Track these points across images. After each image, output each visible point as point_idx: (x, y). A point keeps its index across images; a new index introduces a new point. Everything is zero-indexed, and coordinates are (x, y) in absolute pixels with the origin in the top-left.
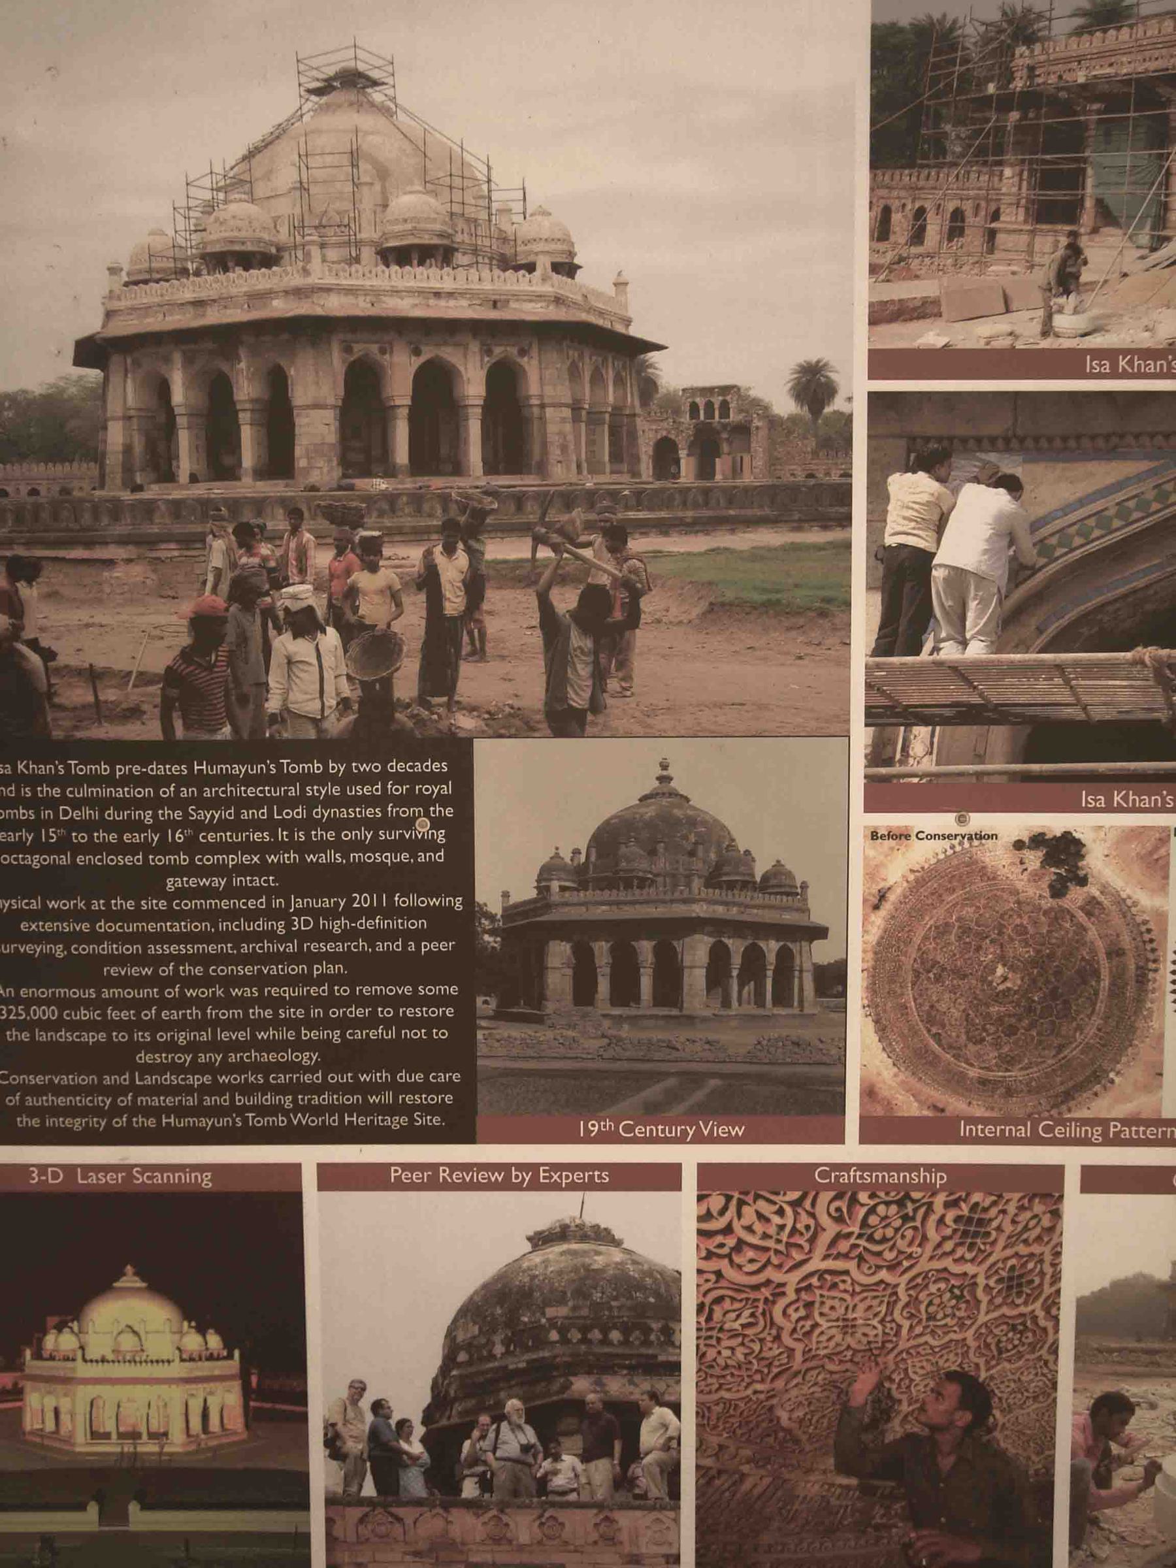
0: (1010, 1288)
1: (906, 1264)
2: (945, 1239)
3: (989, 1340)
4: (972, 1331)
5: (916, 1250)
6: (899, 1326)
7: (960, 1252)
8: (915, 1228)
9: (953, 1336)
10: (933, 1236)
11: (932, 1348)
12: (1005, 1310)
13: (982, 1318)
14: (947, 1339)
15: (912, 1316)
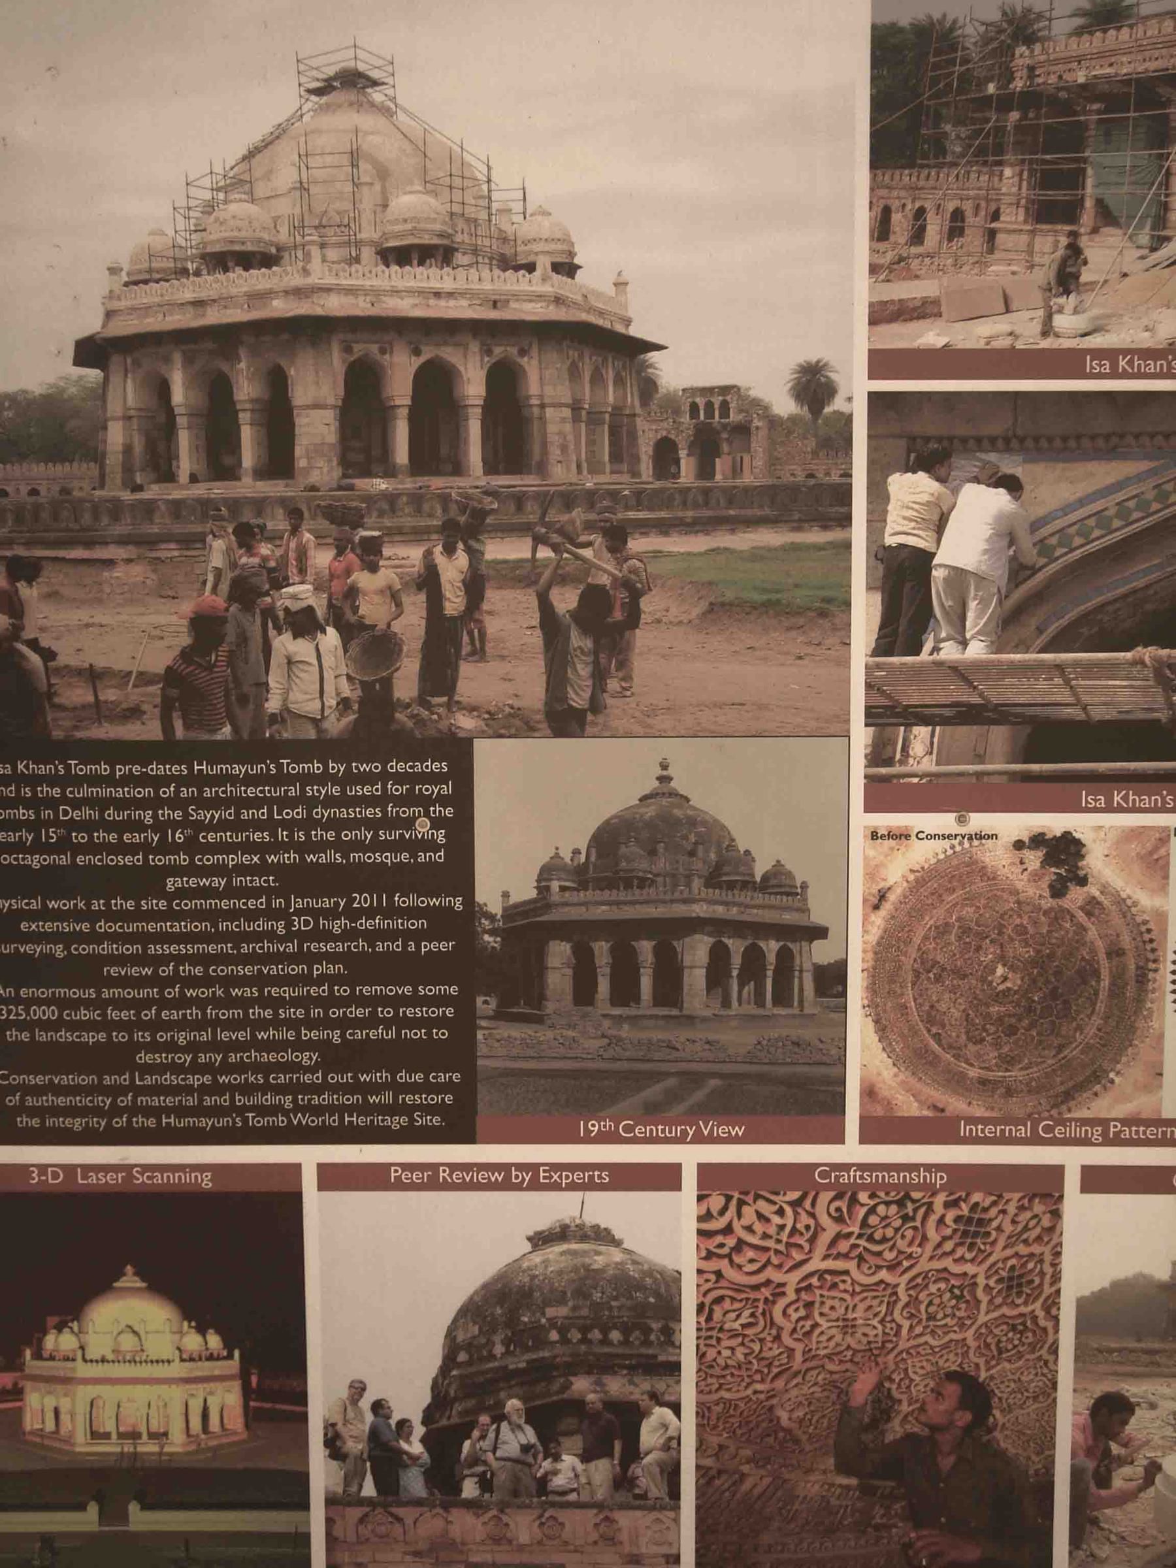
0: (1010, 1288)
1: (906, 1264)
2: (945, 1239)
3: (989, 1340)
4: (972, 1331)
5: (916, 1250)
6: (899, 1326)
7: (960, 1252)
8: (915, 1228)
9: (953, 1336)
10: (933, 1236)
11: (932, 1348)
12: (1005, 1310)
13: (982, 1318)
14: (947, 1339)
15: (912, 1316)
